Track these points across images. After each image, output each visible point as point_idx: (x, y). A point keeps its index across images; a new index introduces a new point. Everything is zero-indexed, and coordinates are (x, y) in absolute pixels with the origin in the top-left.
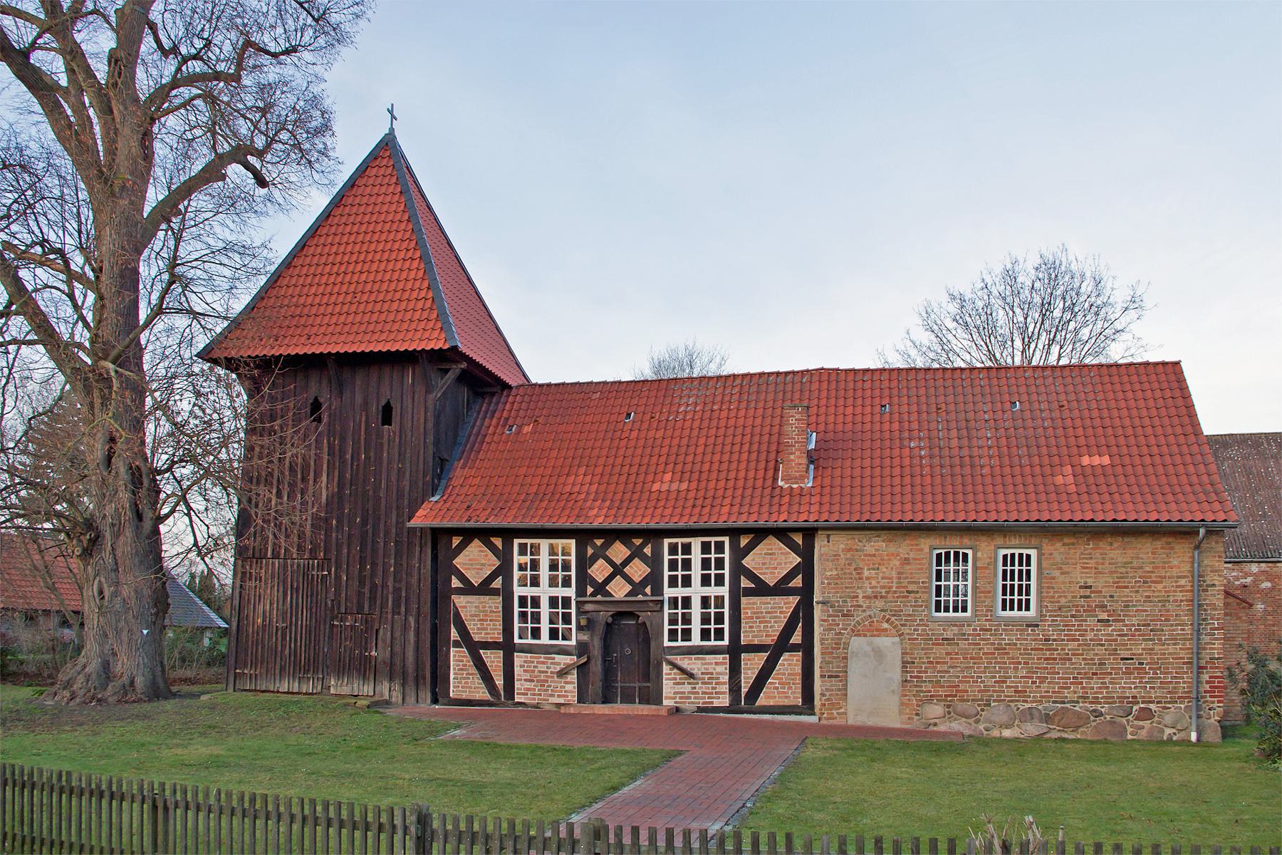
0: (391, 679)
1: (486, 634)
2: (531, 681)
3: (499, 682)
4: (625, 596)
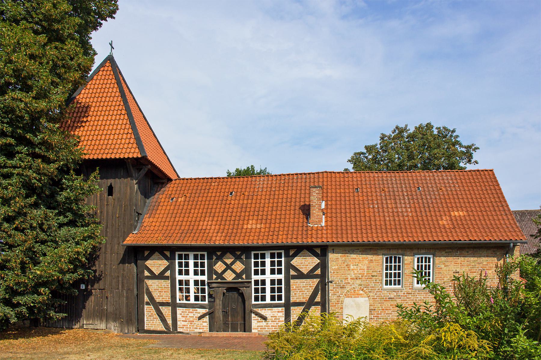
2: (186, 321)
3: (170, 322)
4: (232, 280)
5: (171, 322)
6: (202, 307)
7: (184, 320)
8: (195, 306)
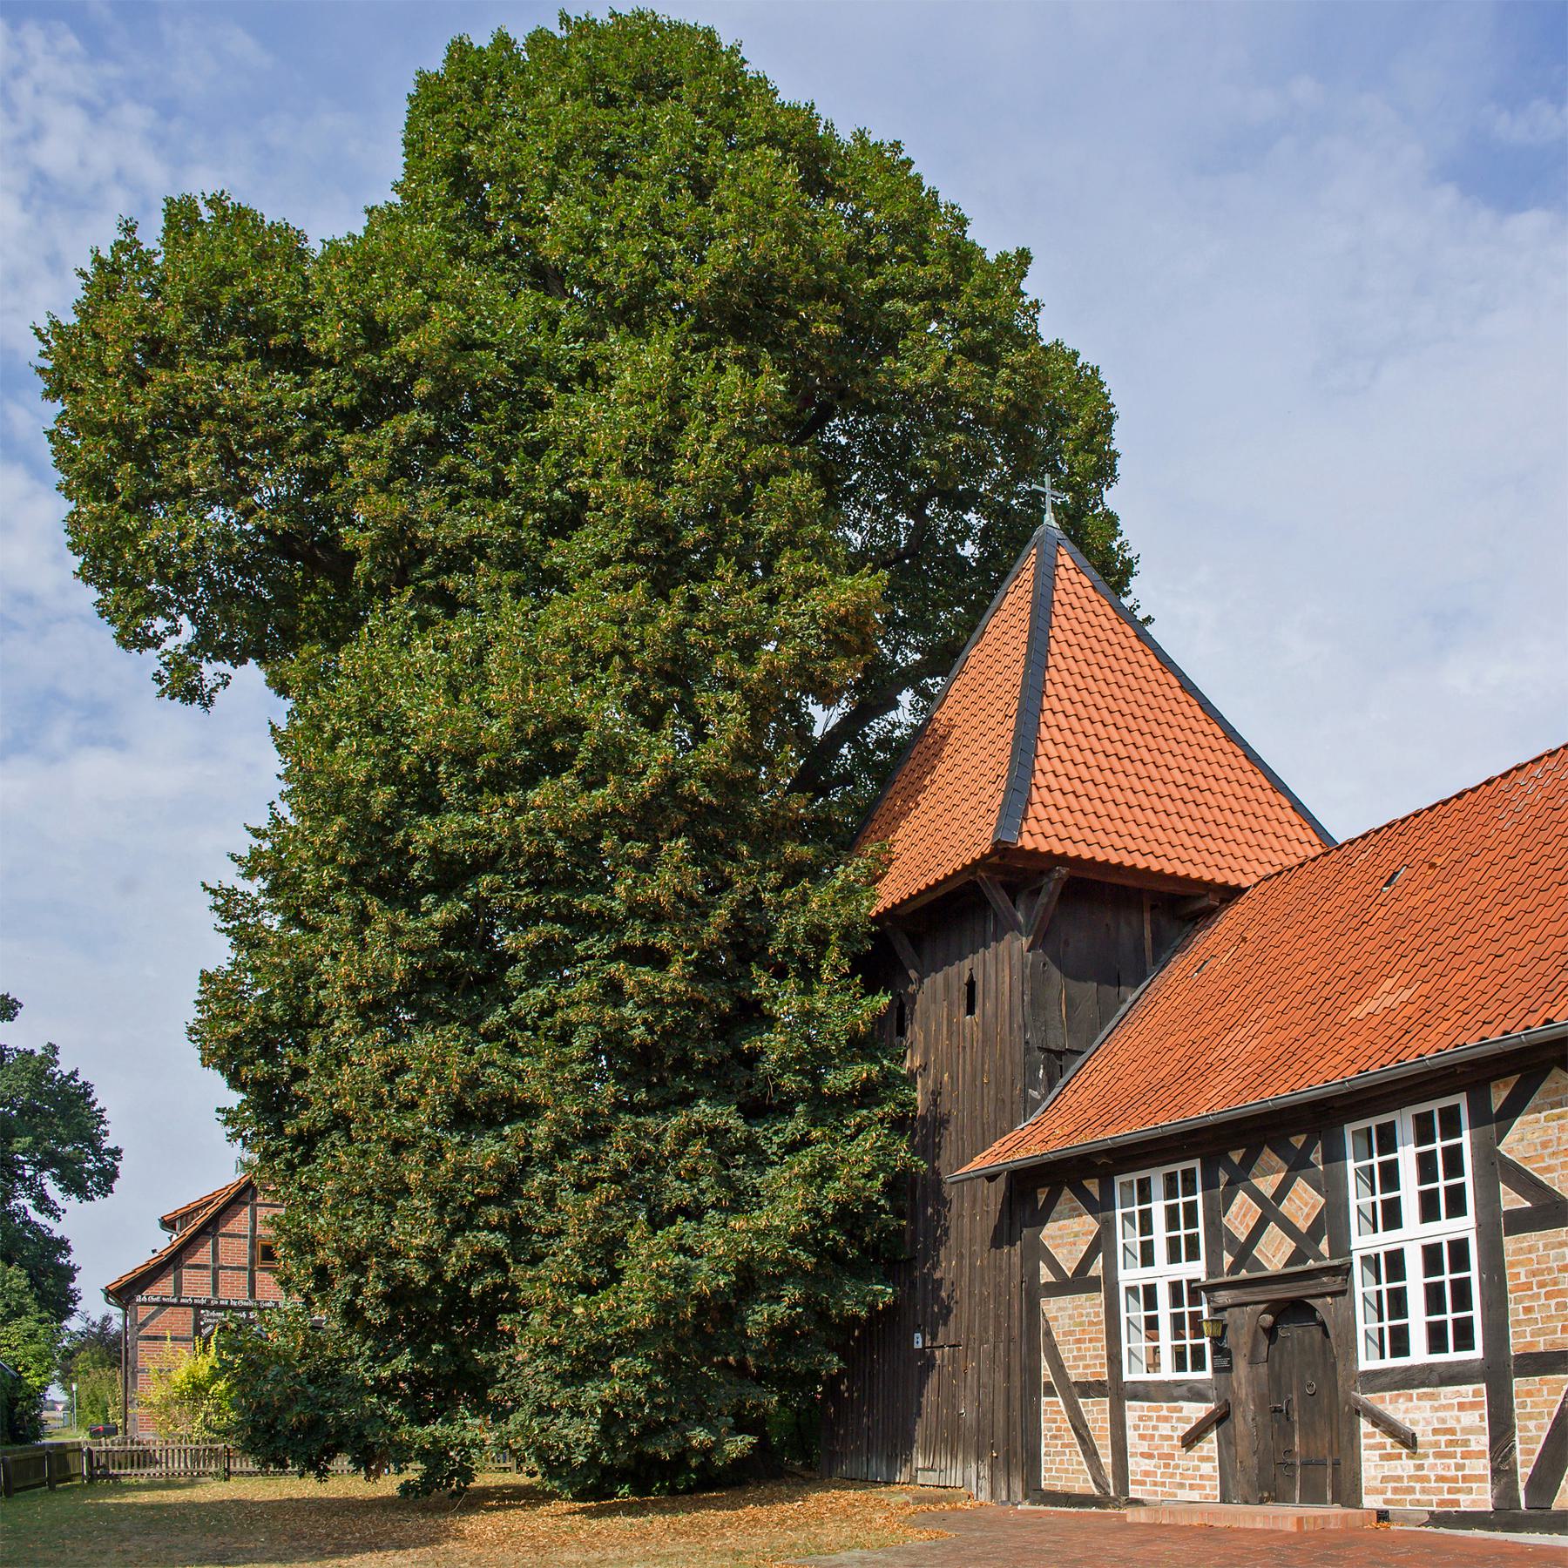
0: (979, 1458)
1: (1086, 1366)
2: (1150, 1456)
3: (1106, 1459)
4: (1286, 1266)
5: (1110, 1460)
6: (1195, 1394)
7: (1146, 1450)
8: (1177, 1392)
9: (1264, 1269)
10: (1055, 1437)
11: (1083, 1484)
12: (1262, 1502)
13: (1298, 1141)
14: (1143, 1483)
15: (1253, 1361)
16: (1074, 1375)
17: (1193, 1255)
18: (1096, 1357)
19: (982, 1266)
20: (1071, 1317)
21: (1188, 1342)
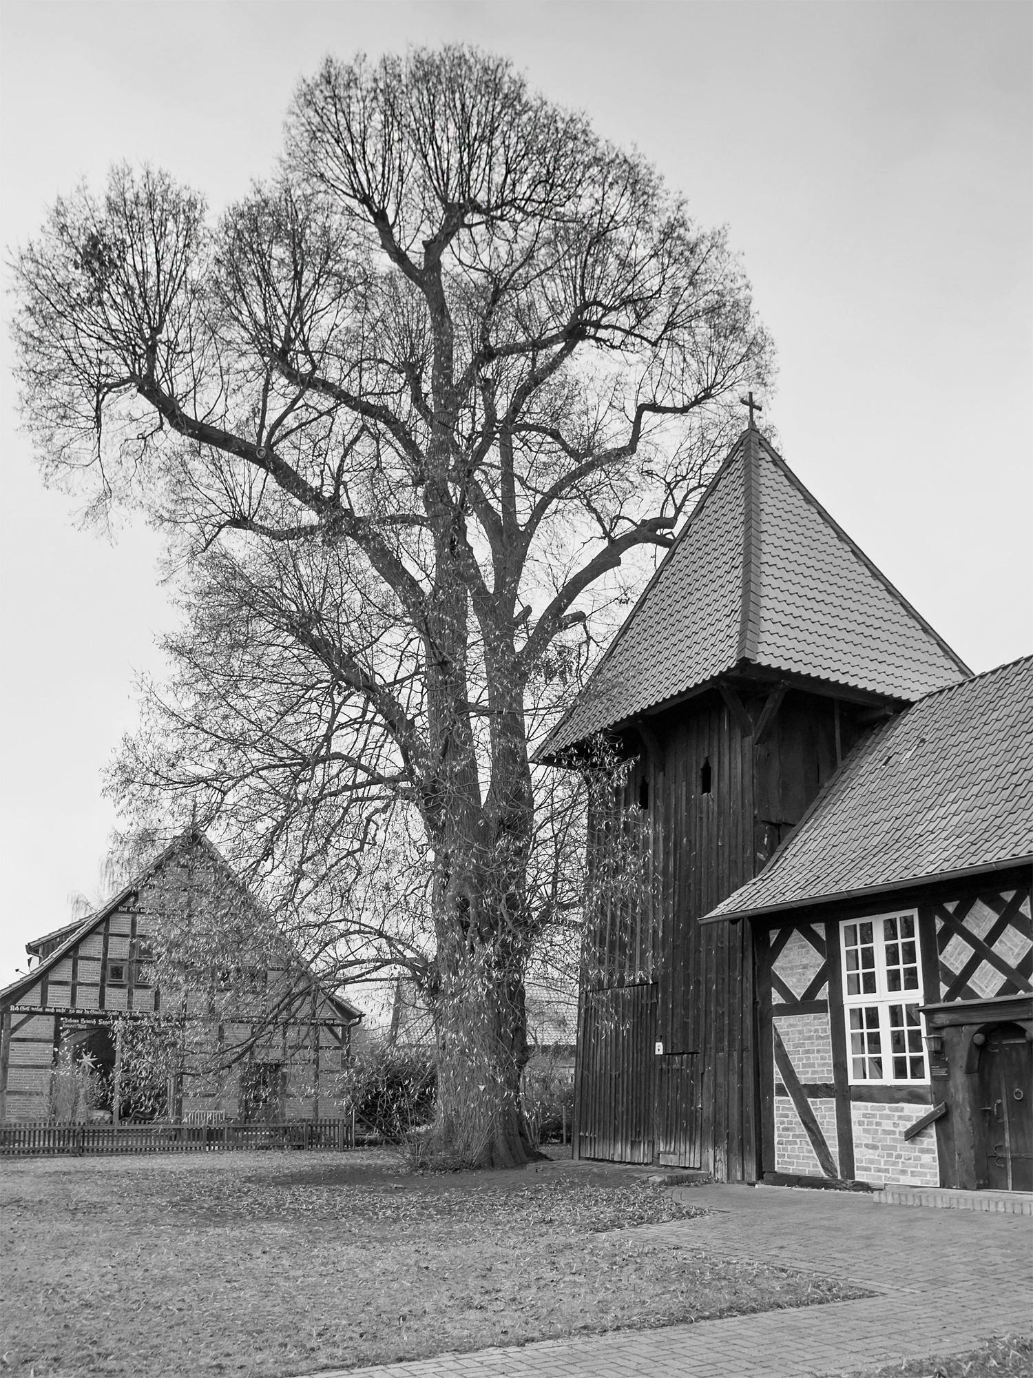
1: (814, 1072)
2: (874, 1147)
3: (834, 1148)
4: (998, 994)
5: (837, 1149)
6: (914, 1096)
7: (870, 1142)
8: (898, 1095)
9: (978, 997)
10: (786, 1129)
11: (811, 1166)
12: (979, 1188)
13: (1008, 896)
14: (867, 1169)
15: (969, 1071)
16: (803, 1079)
17: (911, 984)
18: (824, 1065)
19: (717, 990)
20: (800, 1032)
21: (908, 1054)
